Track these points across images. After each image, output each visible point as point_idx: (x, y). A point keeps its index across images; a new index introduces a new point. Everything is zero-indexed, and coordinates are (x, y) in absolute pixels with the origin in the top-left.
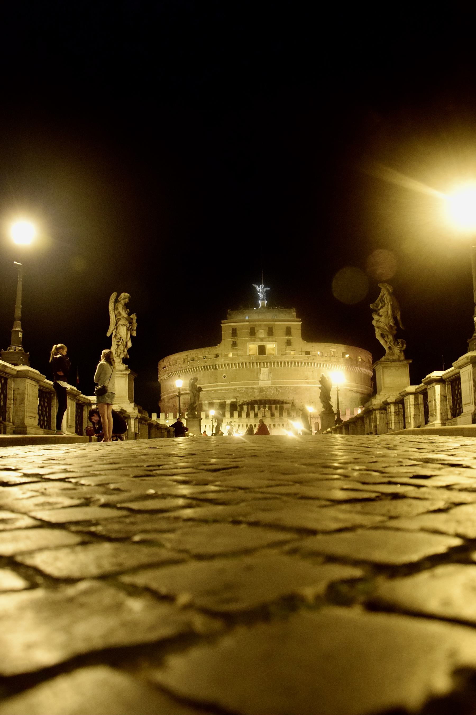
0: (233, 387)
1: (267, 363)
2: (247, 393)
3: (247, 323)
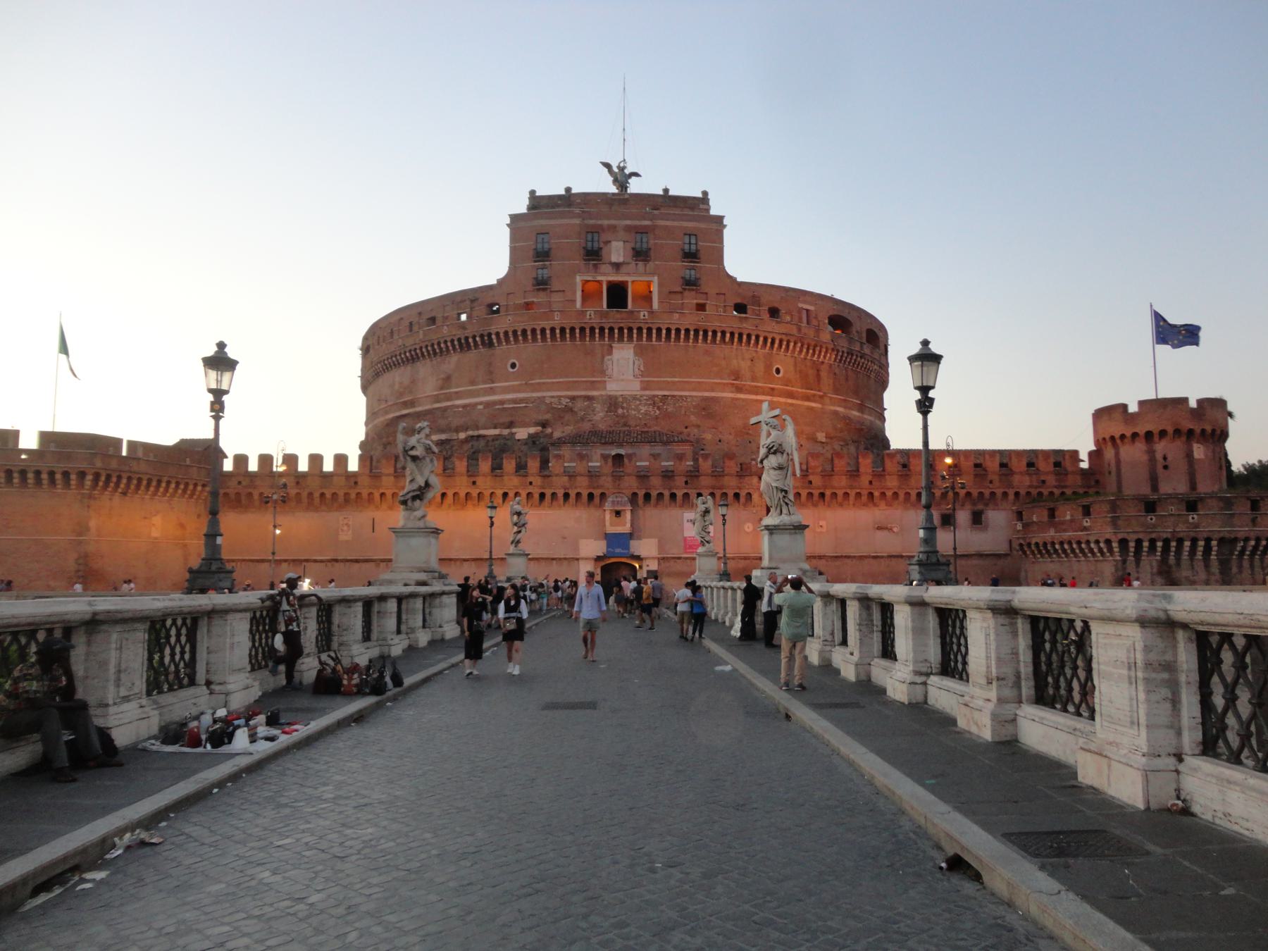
0: (535, 395)
1: (630, 329)
2: (571, 410)
3: (577, 221)
